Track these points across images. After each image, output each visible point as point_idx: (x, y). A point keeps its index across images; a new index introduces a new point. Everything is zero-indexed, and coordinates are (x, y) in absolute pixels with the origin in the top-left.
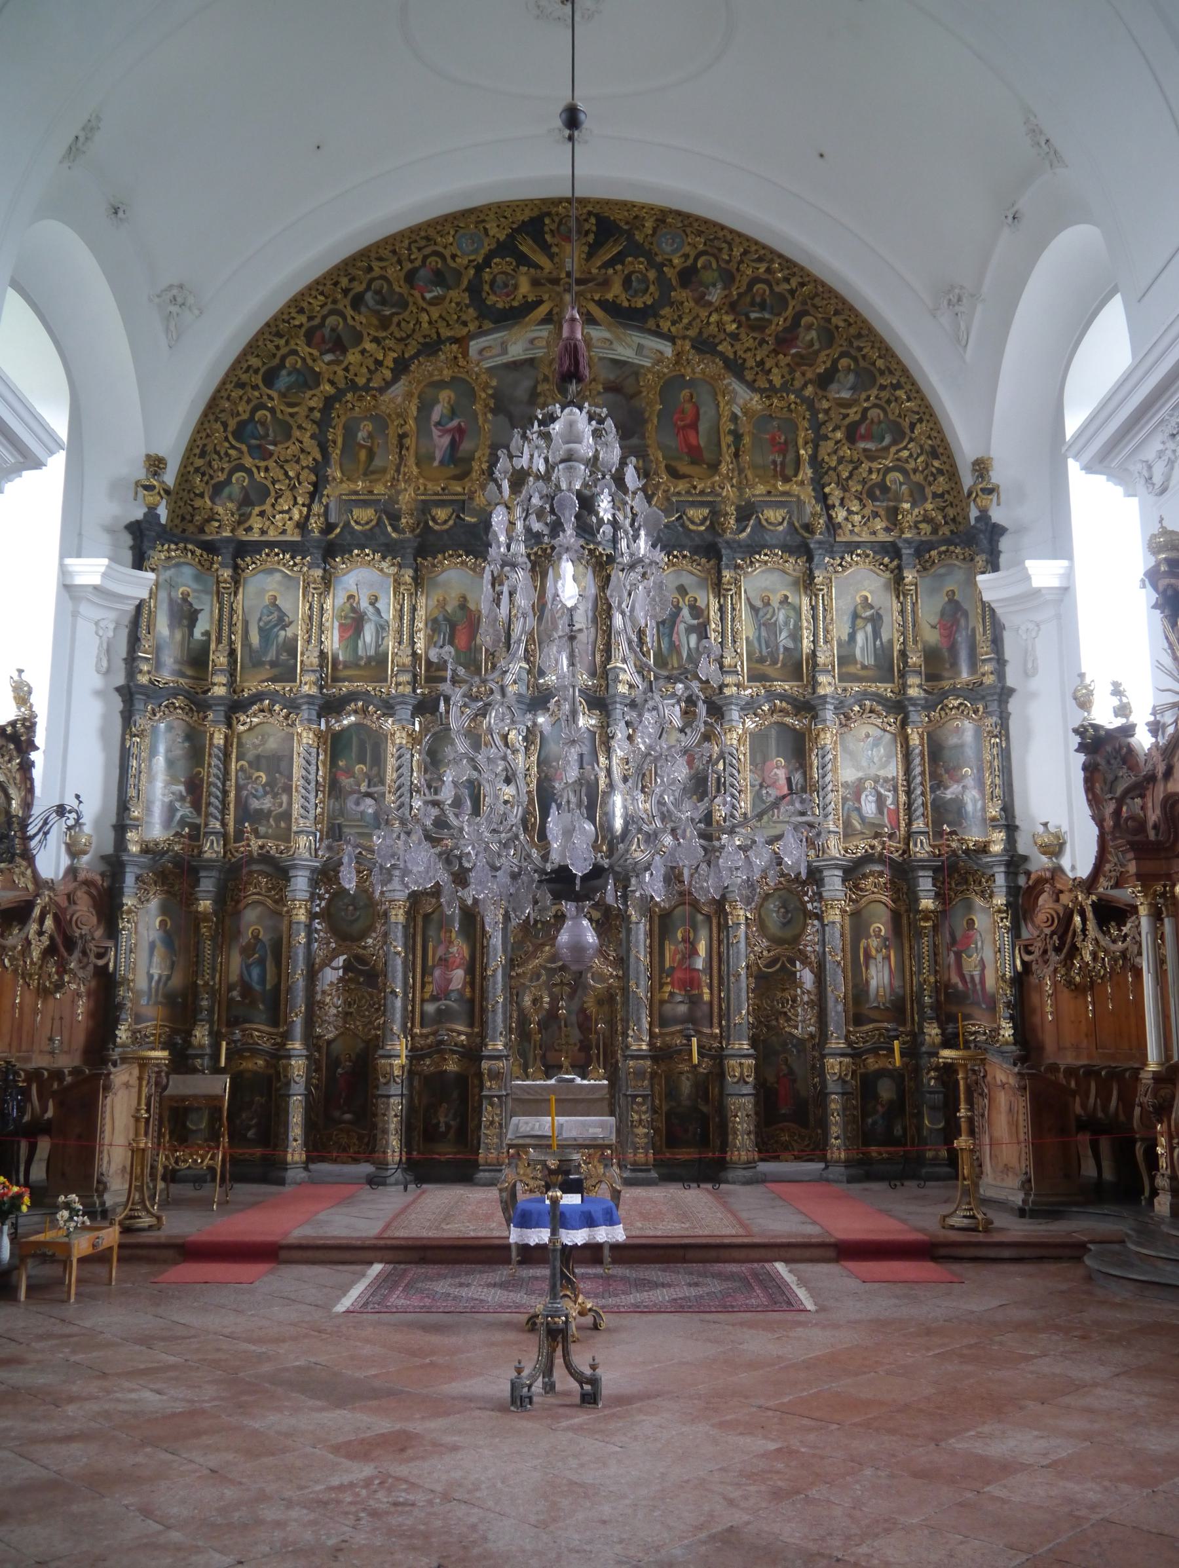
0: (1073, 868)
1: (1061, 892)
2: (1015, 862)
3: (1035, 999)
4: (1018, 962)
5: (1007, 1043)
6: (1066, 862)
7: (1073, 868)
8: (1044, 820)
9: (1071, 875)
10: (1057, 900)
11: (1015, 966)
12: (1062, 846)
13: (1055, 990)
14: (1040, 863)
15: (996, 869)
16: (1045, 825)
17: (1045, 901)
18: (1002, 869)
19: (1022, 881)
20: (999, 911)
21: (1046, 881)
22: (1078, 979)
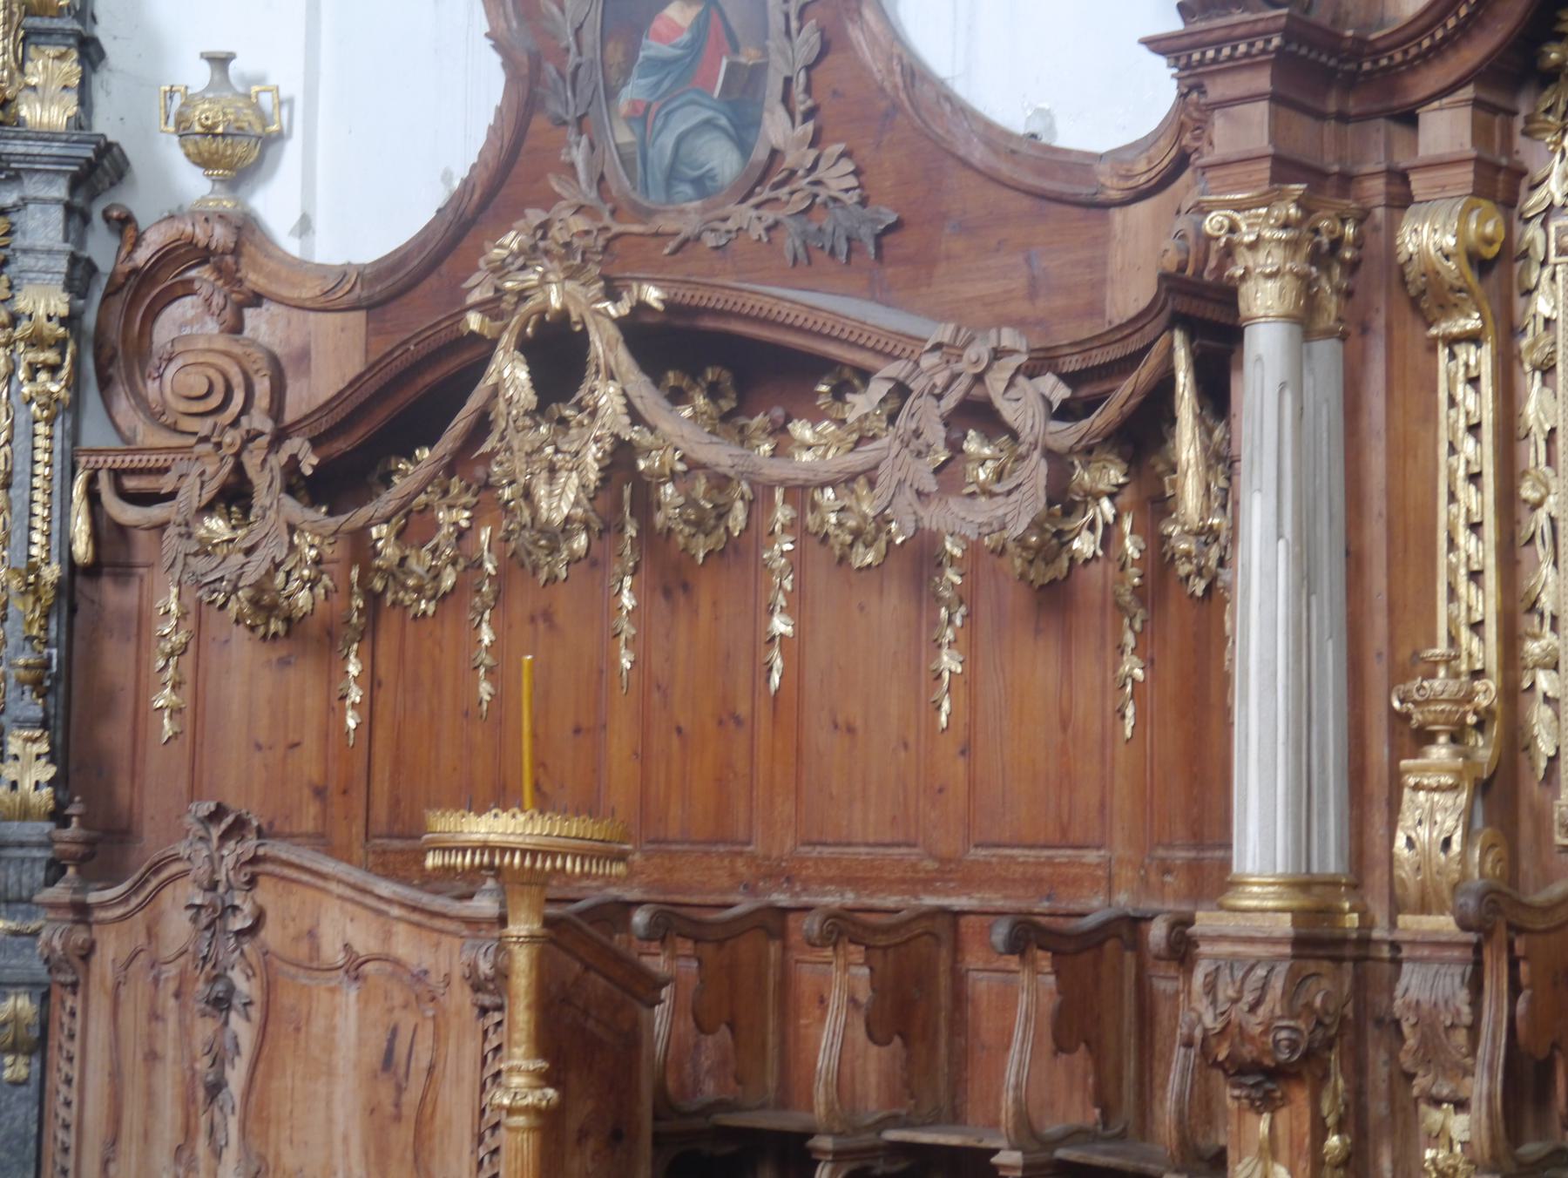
0: (305, 226)
1: (256, 299)
2: (97, 171)
3: (116, 660)
4: (80, 527)
5: (25, 813)
6: (274, 204)
7: (305, 226)
8: (219, 47)
9: (292, 246)
10: (237, 328)
11: (67, 543)
12: (270, 142)
13: (197, 633)
14: (173, 186)
15: (32, 187)
16: (220, 62)
17: (185, 321)
18: (60, 190)
19: (102, 249)
20: (36, 341)
21: (204, 255)
22: (303, 598)
